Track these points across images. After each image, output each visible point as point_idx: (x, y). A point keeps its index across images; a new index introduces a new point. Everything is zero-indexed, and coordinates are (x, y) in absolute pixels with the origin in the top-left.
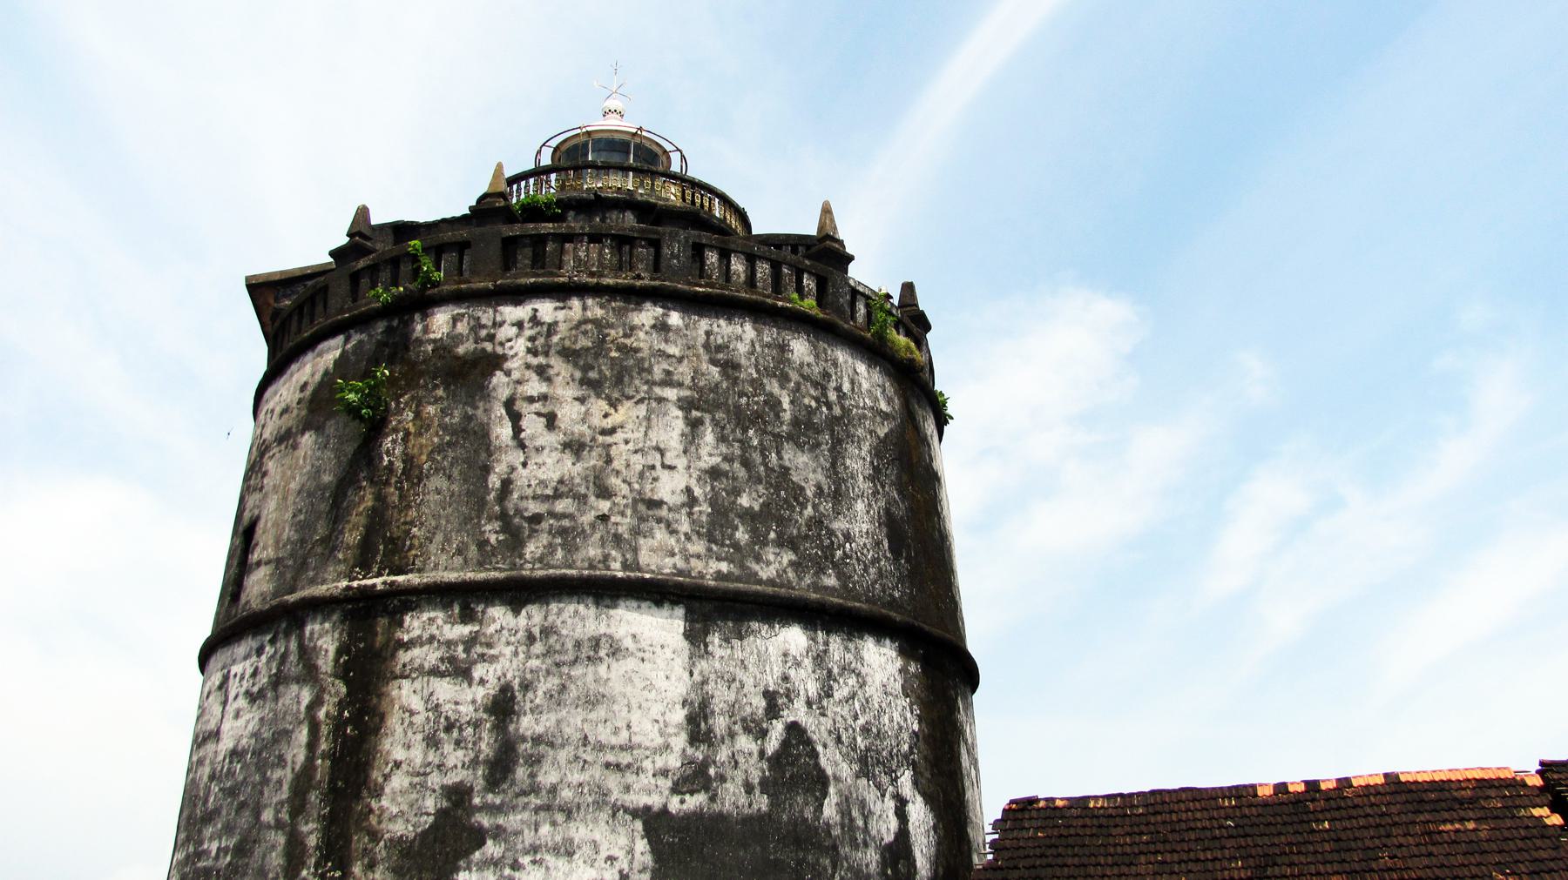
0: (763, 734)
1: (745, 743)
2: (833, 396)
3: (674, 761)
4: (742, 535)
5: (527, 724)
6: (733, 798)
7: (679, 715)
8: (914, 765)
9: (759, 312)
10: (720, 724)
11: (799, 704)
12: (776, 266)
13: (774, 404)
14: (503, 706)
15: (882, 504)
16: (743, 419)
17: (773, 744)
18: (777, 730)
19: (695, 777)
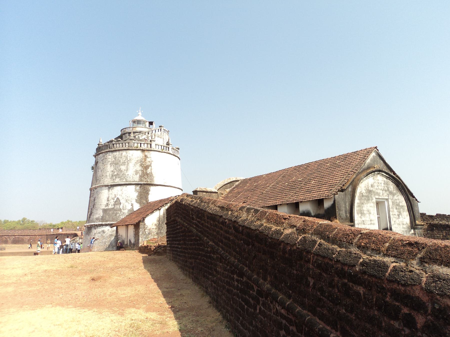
0: (114, 199)
1: (112, 201)
2: (128, 158)
3: (105, 203)
4: (114, 178)
5: (96, 201)
6: (110, 207)
7: (106, 199)
8: (136, 200)
9: (119, 150)
10: (110, 199)
11: (119, 195)
12: (122, 144)
13: (120, 161)
14: (94, 200)
15: (135, 169)
16: (116, 164)
17: (115, 200)
18: (116, 199)
19: (107, 205)
